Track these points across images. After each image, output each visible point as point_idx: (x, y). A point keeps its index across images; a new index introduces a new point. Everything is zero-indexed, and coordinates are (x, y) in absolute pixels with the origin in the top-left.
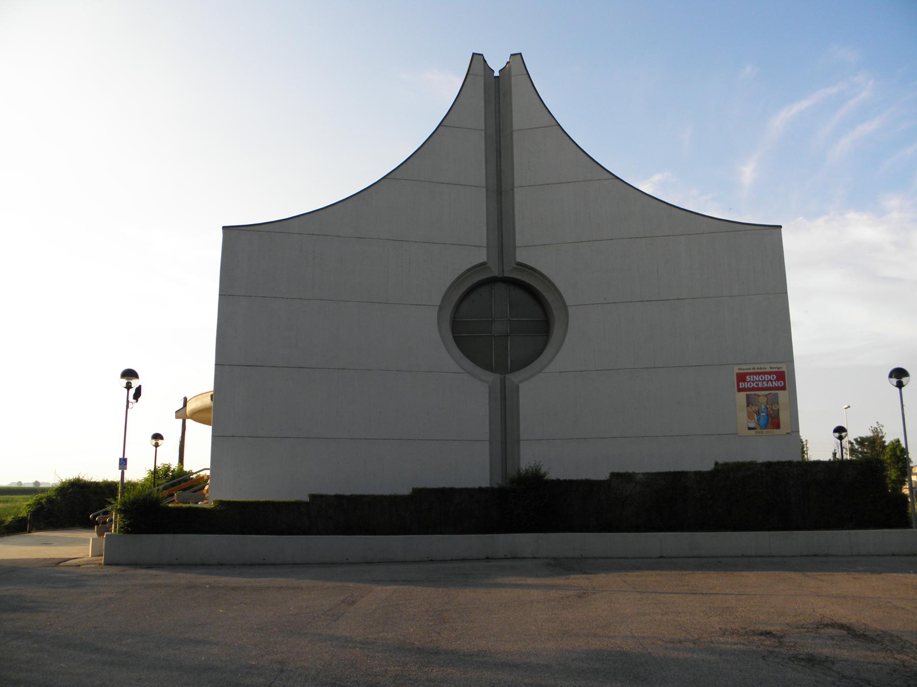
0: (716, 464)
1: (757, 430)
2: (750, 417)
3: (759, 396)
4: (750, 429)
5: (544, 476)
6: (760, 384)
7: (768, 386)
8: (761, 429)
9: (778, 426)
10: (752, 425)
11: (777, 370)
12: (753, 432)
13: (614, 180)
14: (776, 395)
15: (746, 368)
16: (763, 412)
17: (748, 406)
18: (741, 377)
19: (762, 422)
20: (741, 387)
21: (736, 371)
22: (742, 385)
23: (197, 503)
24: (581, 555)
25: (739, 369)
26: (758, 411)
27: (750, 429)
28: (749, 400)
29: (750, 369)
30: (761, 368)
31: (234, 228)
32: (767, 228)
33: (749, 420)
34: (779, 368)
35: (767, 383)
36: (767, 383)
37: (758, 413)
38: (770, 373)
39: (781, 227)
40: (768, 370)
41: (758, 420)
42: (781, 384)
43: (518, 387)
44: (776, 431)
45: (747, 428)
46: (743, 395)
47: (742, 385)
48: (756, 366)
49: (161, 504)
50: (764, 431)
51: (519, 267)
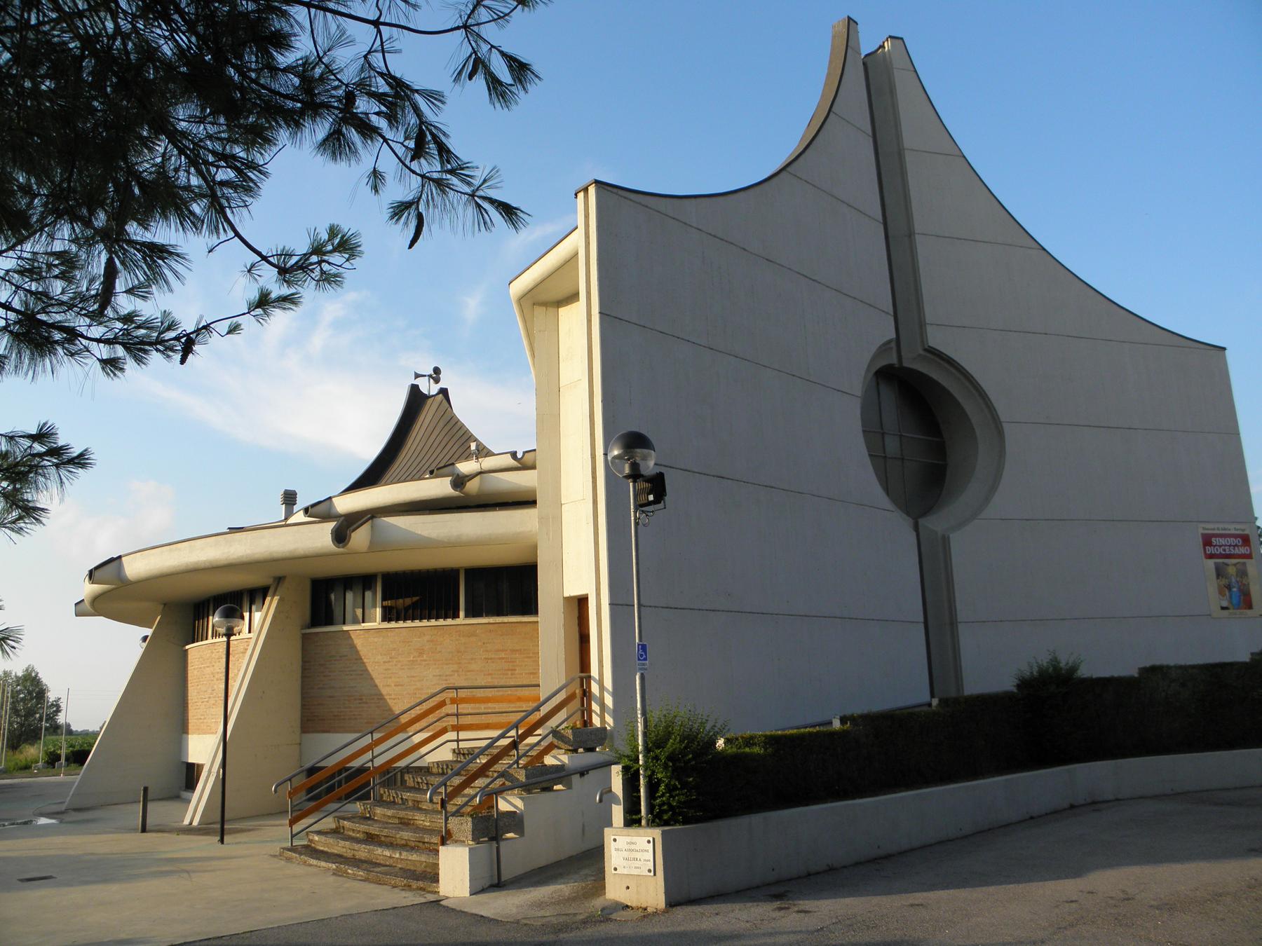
0: (1252, 654)
1: (1231, 611)
2: (1221, 593)
3: (1227, 565)
4: (1223, 608)
5: (1073, 669)
6: (1227, 550)
7: (1218, 553)
8: (1234, 609)
9: (1249, 606)
10: (1225, 604)
11: (1241, 532)
12: (1226, 612)
13: (1040, 251)
14: (1244, 564)
15: (1212, 528)
16: (1234, 587)
17: (1218, 578)
18: (1207, 541)
19: (1235, 601)
20: (1207, 552)
21: (1201, 531)
22: (1210, 550)
23: (191, 774)
24: (1172, 790)
25: (1204, 529)
26: (1229, 585)
27: (1223, 608)
28: (1220, 573)
29: (1214, 529)
30: (1225, 529)
31: (620, 192)
32: (1212, 348)
33: (1221, 597)
34: (1243, 530)
35: (1234, 549)
36: (1234, 549)
37: (1229, 587)
38: (1235, 536)
39: (1224, 349)
40: (1233, 532)
41: (1231, 597)
42: (1247, 550)
43: (945, 541)
44: (1249, 612)
45: (1220, 608)
46: (1211, 563)
47: (1210, 550)
48: (1221, 526)
49: (1035, 673)
50: (1238, 611)
51: (928, 355)
